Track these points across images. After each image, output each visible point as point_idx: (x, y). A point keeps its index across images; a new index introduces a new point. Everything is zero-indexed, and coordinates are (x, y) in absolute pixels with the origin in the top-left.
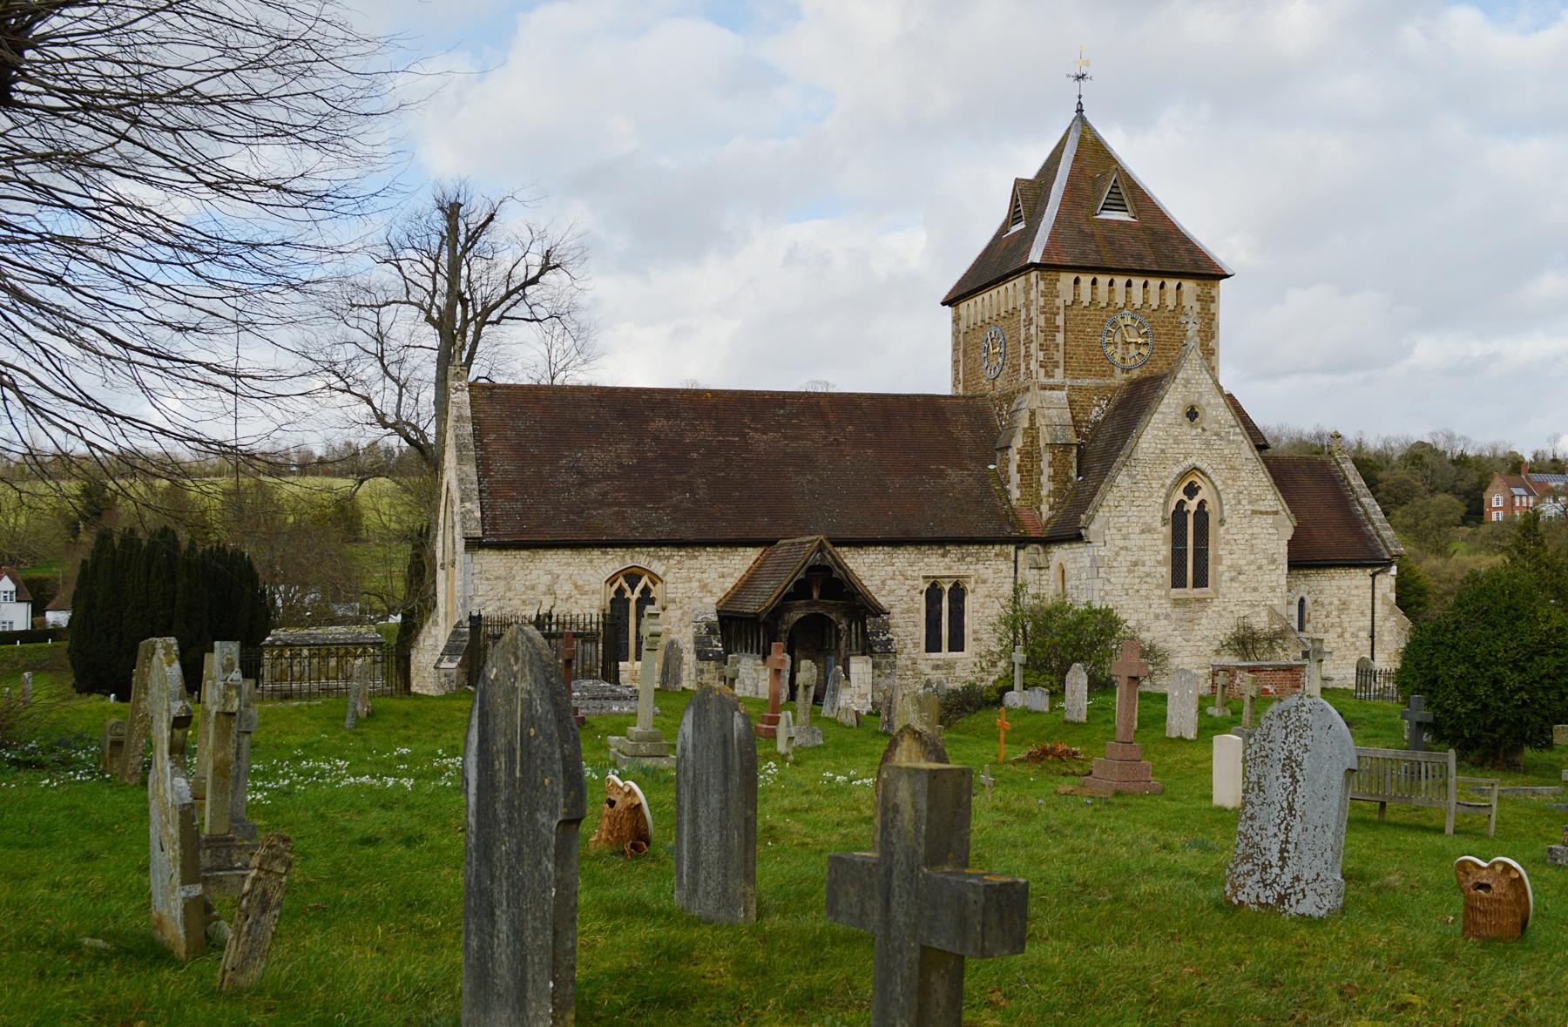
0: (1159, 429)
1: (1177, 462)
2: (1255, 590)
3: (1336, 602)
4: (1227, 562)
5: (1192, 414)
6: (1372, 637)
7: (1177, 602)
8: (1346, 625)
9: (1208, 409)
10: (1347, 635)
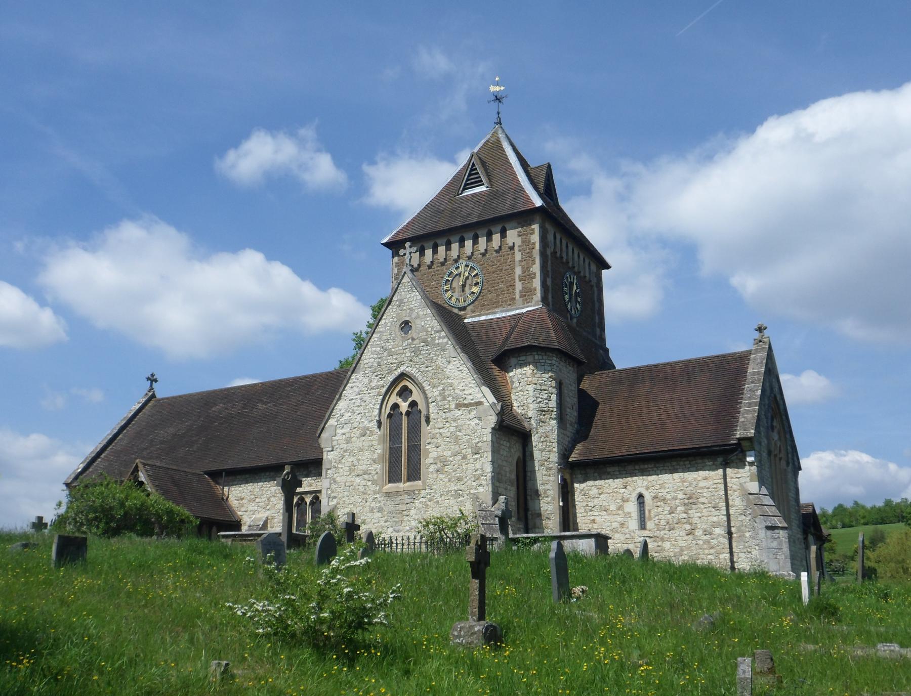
0: (377, 345)
1: (390, 372)
2: (459, 479)
4: (433, 455)
5: (406, 326)
6: (730, 533)
7: (388, 494)
8: (695, 520)
9: (418, 321)
10: (698, 533)
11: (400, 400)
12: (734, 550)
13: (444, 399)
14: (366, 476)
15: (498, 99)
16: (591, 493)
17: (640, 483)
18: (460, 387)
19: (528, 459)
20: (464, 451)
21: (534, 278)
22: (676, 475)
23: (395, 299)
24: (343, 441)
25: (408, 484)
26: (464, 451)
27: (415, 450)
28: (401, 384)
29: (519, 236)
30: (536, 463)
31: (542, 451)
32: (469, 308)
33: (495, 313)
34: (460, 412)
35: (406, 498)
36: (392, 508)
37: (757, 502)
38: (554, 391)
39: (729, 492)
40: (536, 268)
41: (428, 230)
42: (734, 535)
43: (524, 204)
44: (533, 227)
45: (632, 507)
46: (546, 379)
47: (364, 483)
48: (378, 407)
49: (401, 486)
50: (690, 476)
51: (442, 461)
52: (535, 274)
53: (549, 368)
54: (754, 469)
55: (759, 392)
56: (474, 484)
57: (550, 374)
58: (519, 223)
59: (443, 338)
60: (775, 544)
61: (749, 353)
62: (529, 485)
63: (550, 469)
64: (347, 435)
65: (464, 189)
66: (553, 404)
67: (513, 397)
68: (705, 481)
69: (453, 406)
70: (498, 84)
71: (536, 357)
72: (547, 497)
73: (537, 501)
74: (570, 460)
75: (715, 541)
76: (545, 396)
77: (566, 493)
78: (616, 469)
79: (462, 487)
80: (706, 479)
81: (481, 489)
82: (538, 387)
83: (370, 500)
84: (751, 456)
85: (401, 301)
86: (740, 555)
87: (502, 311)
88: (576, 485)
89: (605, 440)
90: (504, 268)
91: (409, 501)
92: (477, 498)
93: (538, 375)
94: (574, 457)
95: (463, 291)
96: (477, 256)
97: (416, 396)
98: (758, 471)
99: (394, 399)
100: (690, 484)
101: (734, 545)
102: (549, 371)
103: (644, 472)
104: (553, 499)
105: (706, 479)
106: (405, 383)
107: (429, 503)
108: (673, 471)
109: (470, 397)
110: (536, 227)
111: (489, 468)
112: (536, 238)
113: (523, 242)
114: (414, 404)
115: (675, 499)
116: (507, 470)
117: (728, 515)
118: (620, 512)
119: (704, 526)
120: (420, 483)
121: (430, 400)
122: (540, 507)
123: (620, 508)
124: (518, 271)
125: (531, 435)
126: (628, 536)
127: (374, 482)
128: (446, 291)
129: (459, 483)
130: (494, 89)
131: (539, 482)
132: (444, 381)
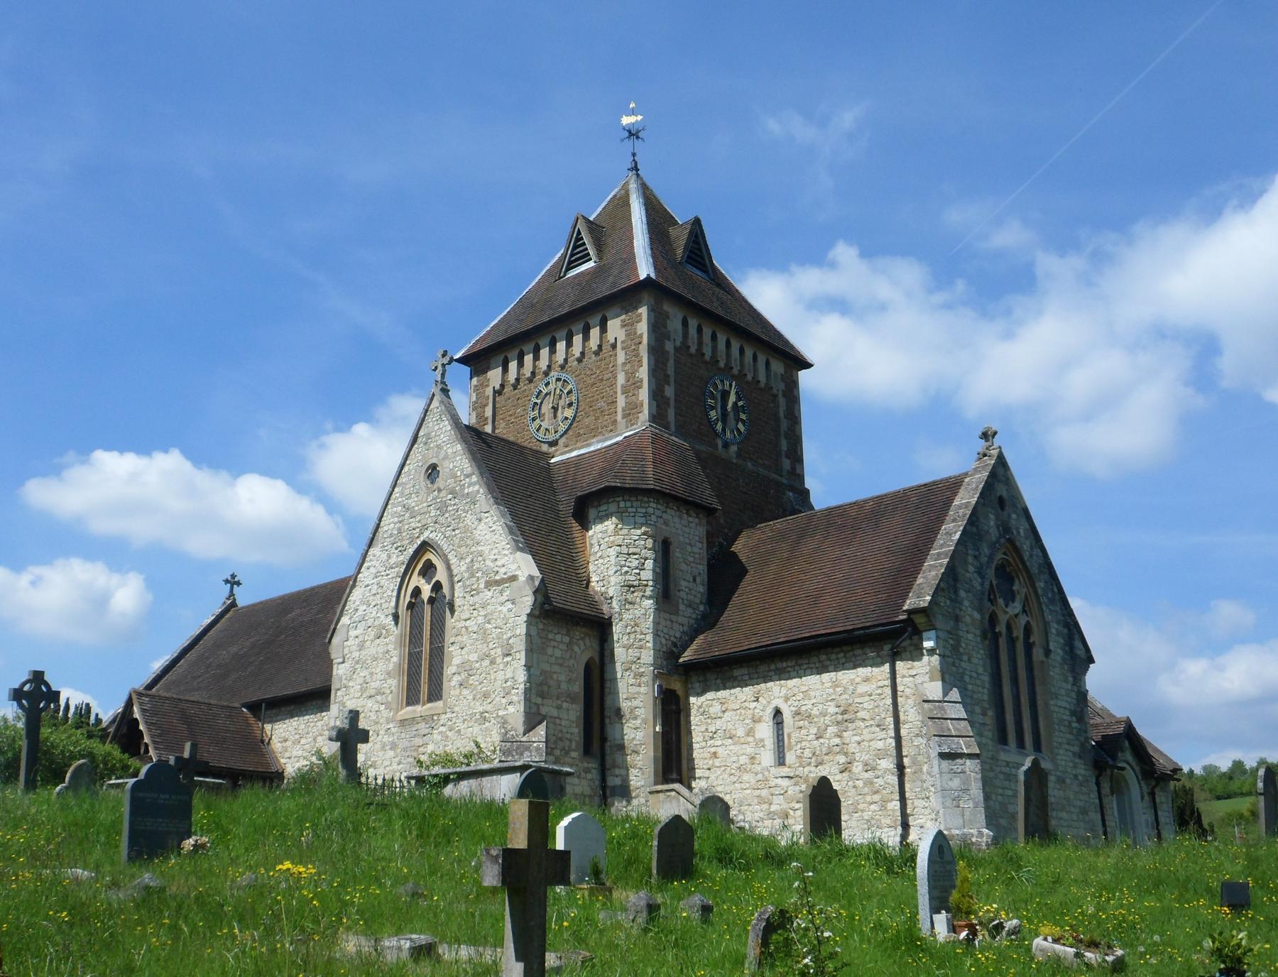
3: (832, 710)
5: (432, 472)
6: (901, 768)
7: (403, 723)
8: (852, 748)
9: (446, 464)
10: (857, 768)
11: (423, 581)
12: (907, 795)
13: (472, 576)
14: (379, 698)
15: (633, 134)
16: (712, 710)
17: (778, 692)
18: (492, 557)
19: (607, 660)
20: (493, 652)
21: (640, 387)
22: (826, 676)
23: (421, 433)
24: (355, 648)
25: (410, 708)
26: (493, 652)
27: (438, 655)
28: (421, 559)
29: (623, 326)
30: (618, 667)
31: (628, 647)
32: (561, 442)
33: (589, 445)
34: (490, 594)
35: (422, 727)
36: (407, 744)
37: (935, 713)
38: (650, 554)
39: (900, 699)
40: (643, 373)
41: (511, 333)
42: (908, 770)
43: (628, 278)
44: (640, 311)
45: (765, 731)
46: (638, 539)
47: (376, 707)
48: (395, 594)
49: (419, 709)
50: (846, 676)
51: (467, 668)
52: (641, 381)
53: (643, 520)
54: (936, 659)
55: (957, 536)
56: (504, 701)
57: (644, 529)
58: (623, 308)
59: (474, 484)
60: (956, 783)
61: (966, 475)
62: (608, 702)
63: (641, 675)
64: (361, 638)
65: (568, 269)
66: (647, 575)
67: (591, 568)
68: (863, 682)
69: (482, 586)
70: (633, 113)
71: (622, 504)
72: (635, 718)
73: (618, 726)
74: (681, 660)
75: (880, 781)
76: (635, 563)
77: (672, 714)
78: (745, 671)
79: (489, 708)
80: (867, 680)
81: (511, 709)
82: (625, 550)
83: (382, 732)
84: (929, 639)
85: (428, 436)
86: (917, 802)
87: (598, 442)
88: (692, 700)
89: (743, 625)
90: (606, 377)
91: (427, 731)
92: (505, 722)
93: (625, 531)
94: (687, 656)
95: (555, 417)
96: (573, 363)
97: (441, 575)
98: (941, 663)
99: (416, 580)
100: (845, 692)
101: (907, 786)
102: (642, 525)
103: (783, 675)
104: (645, 721)
105: (867, 680)
106: (429, 556)
107: (449, 734)
108: (821, 670)
109: (503, 570)
110: (643, 311)
111: (521, 676)
112: (643, 328)
113: (627, 335)
114: (437, 587)
115: (824, 714)
116: (562, 678)
117: (898, 738)
118: (750, 739)
119: (865, 757)
120: (440, 704)
121: (456, 579)
122: (623, 735)
123: (750, 732)
124: (621, 379)
125: (611, 624)
126: (760, 777)
127: (388, 706)
128: (534, 419)
129: (487, 705)
130: (626, 120)
131: (622, 695)
132: (473, 549)
